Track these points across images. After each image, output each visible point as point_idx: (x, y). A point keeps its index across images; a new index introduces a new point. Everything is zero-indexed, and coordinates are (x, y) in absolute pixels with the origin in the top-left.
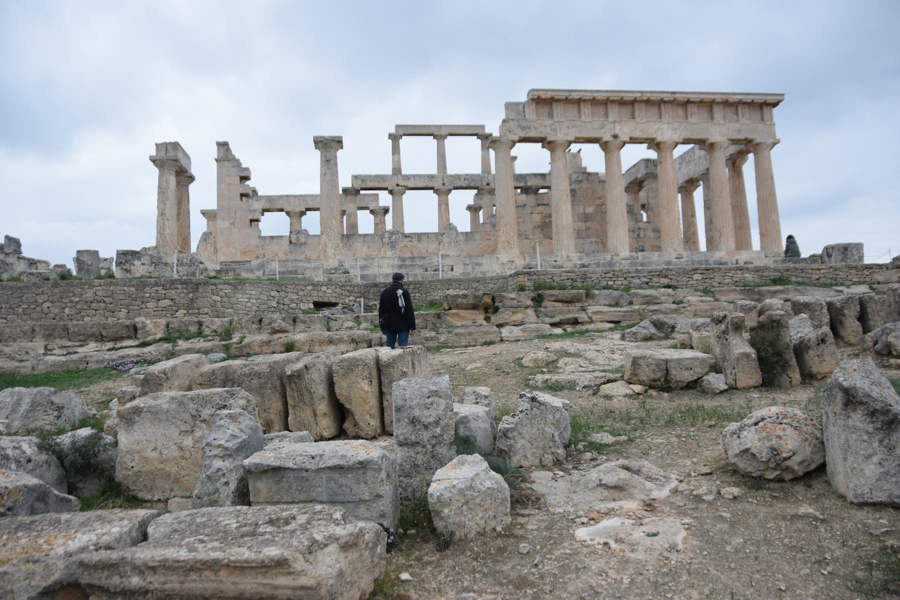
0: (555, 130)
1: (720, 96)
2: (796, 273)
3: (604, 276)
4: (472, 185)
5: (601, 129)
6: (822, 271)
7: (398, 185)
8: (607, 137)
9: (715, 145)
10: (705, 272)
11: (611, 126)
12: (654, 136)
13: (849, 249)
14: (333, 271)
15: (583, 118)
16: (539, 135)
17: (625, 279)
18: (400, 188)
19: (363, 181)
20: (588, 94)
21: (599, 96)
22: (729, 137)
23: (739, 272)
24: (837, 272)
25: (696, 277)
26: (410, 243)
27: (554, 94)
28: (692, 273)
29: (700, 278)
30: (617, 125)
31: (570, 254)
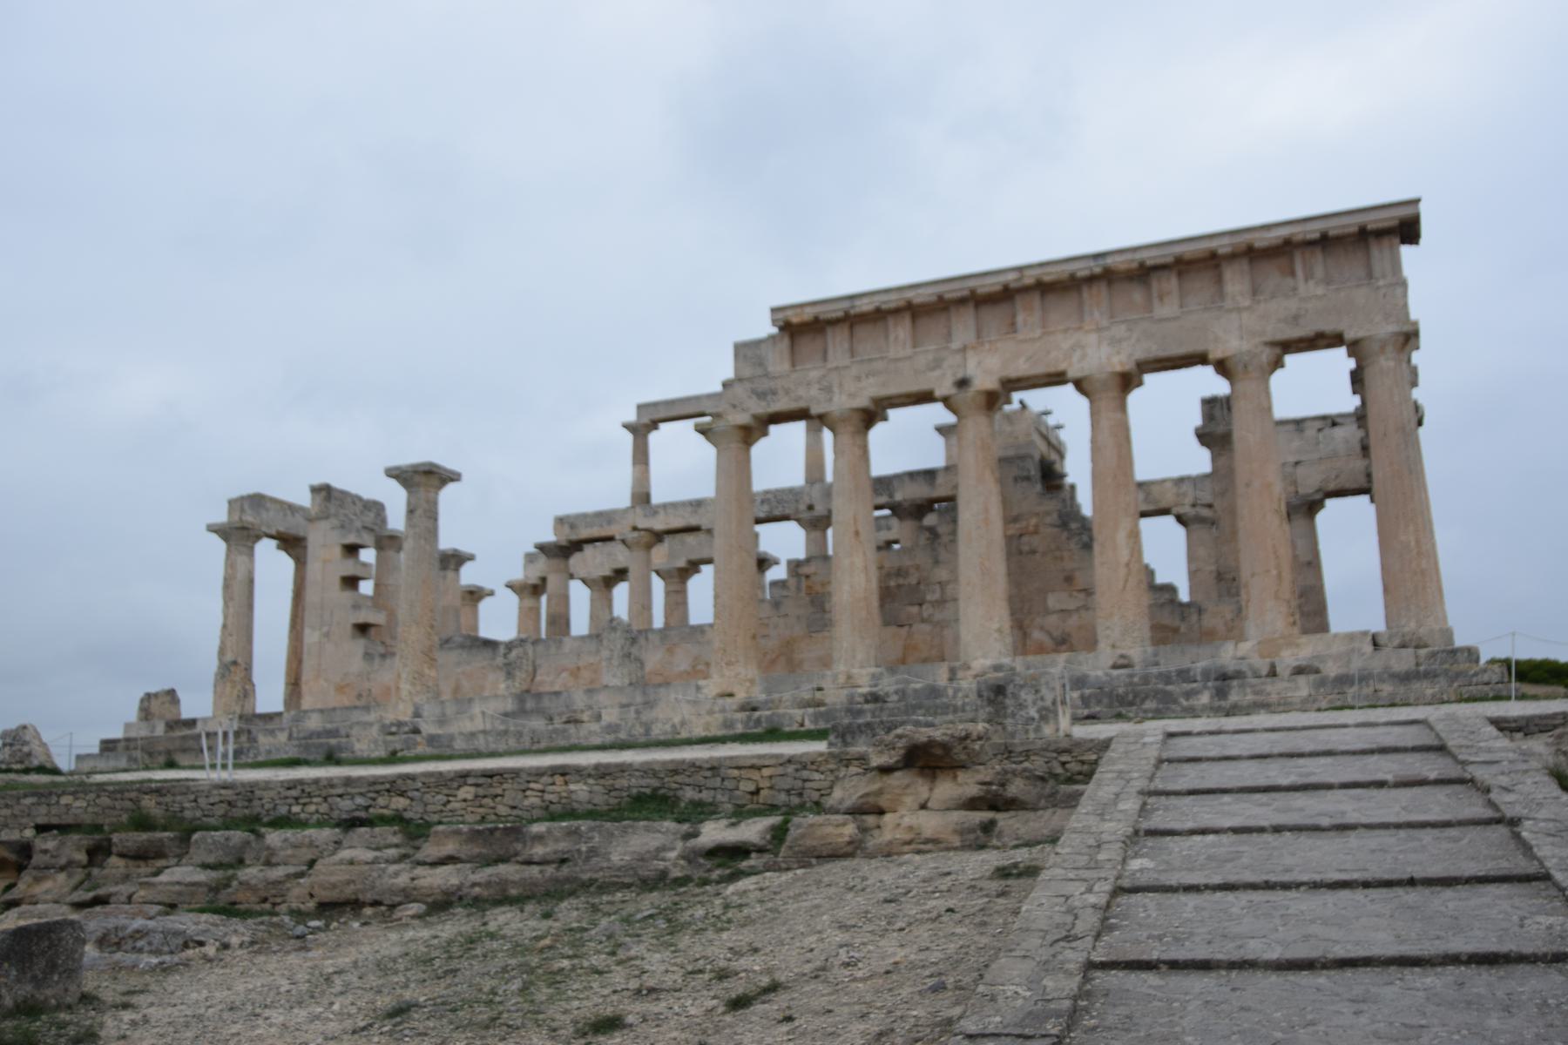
0: (828, 390)
2: (698, 779)
4: (777, 513)
5: (933, 369)
6: (766, 772)
8: (945, 388)
10: (481, 780)
11: (958, 358)
12: (1062, 367)
13: (1010, 689)
14: (394, 729)
18: (636, 534)
19: (573, 527)
20: (893, 297)
21: (919, 297)
22: (1268, 338)
23: (559, 779)
24: (805, 774)
25: (466, 792)
28: (455, 784)
29: (470, 797)
30: (970, 353)
31: (855, 671)
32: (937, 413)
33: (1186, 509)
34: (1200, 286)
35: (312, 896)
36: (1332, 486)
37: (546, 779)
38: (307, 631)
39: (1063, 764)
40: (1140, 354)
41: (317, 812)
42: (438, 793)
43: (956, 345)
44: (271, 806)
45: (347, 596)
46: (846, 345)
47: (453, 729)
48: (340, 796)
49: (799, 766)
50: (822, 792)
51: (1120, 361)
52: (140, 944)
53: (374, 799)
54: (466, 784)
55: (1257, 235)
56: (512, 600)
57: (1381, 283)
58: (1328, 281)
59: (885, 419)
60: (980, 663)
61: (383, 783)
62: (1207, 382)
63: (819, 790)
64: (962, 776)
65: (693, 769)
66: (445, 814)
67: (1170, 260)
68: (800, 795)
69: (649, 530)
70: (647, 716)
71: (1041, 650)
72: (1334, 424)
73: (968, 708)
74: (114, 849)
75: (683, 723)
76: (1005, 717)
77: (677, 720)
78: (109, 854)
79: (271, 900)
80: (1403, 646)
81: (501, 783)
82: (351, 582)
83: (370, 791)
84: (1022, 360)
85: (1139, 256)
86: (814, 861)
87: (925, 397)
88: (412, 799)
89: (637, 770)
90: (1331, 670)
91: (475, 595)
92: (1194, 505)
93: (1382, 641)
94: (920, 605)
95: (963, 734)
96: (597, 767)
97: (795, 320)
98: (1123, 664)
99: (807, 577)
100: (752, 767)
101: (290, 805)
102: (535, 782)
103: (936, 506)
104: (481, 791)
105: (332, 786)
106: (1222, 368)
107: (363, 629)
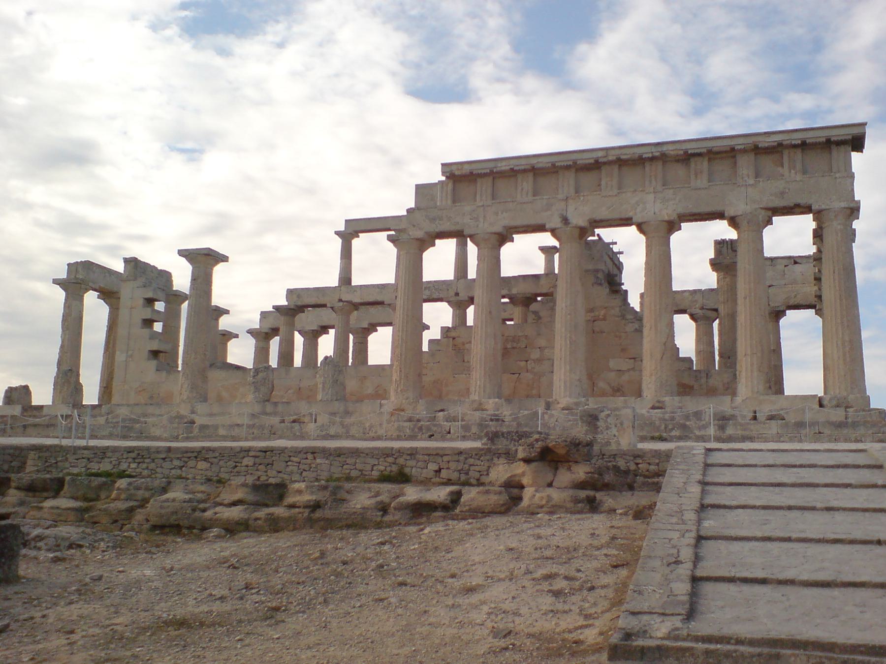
0: (477, 219)
1: (741, 141)
4: (435, 296)
6: (446, 458)
11: (563, 204)
12: (630, 214)
13: (602, 415)
17: (153, 460)
18: (341, 304)
19: (299, 296)
20: (523, 162)
23: (310, 456)
24: (471, 461)
25: (248, 461)
27: (474, 166)
28: (242, 455)
29: (251, 463)
30: (570, 201)
32: (547, 239)
33: (694, 311)
34: (722, 167)
35: (148, 521)
36: (791, 303)
37: (301, 456)
38: (118, 353)
39: (637, 464)
40: (681, 210)
41: (147, 468)
42: (229, 460)
43: (560, 196)
44: (117, 462)
45: (146, 331)
46: (489, 191)
47: (218, 420)
48: (164, 459)
49: (467, 456)
50: (481, 473)
51: (668, 213)
52: (39, 544)
53: (187, 462)
54: (248, 456)
55: (760, 139)
56: (251, 342)
57: (837, 175)
58: (804, 172)
59: (512, 240)
60: (565, 401)
61: (193, 452)
62: (722, 230)
63: (480, 472)
64: (575, 468)
65: (398, 454)
66: (232, 474)
67: (705, 150)
68: (467, 474)
70: (348, 420)
71: (603, 394)
72: (796, 263)
73: (557, 429)
74: (13, 484)
75: (371, 427)
77: (367, 425)
78: (9, 487)
79: (121, 522)
80: (838, 406)
81: (272, 456)
82: (148, 323)
83: (183, 457)
85: (685, 146)
86: (480, 515)
87: (539, 228)
88: (212, 464)
89: (362, 453)
90: (792, 418)
91: (228, 336)
92: (702, 308)
93: (825, 403)
94: (527, 361)
95: (577, 441)
96: (336, 449)
97: (457, 173)
99: (454, 338)
100: (437, 454)
101: (130, 463)
102: (294, 456)
103: (539, 299)
105: (158, 452)
106: (733, 222)
107: (155, 354)
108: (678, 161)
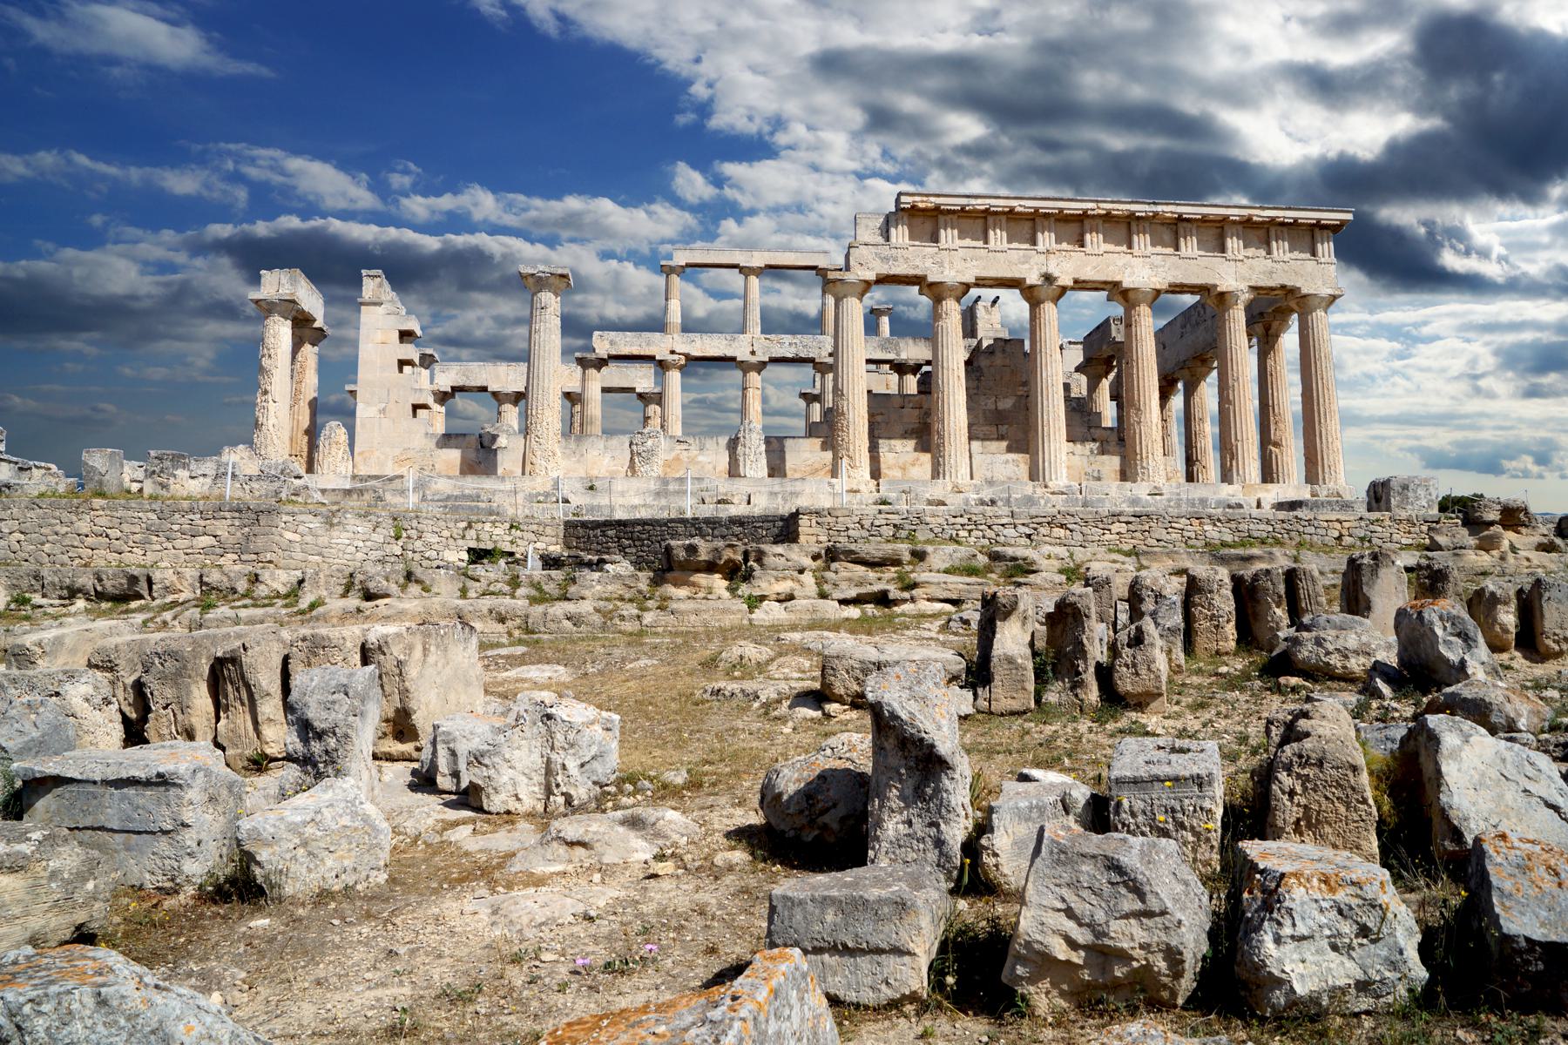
0: (941, 264)
3: (952, 520)
5: (1023, 263)
6: (1346, 525)
7: (673, 352)
8: (1033, 278)
9: (1227, 296)
10: (1133, 519)
12: (1117, 279)
13: (1412, 486)
14: (541, 498)
15: (992, 245)
16: (912, 272)
18: (676, 357)
19: (612, 343)
22: (1253, 283)
24: (1372, 527)
25: (1116, 527)
26: (685, 453)
69: (687, 356)
76: (1407, 503)
84: (1089, 268)
97: (921, 205)
98: (1156, 493)
104: (1132, 527)
108: (1163, 224)
